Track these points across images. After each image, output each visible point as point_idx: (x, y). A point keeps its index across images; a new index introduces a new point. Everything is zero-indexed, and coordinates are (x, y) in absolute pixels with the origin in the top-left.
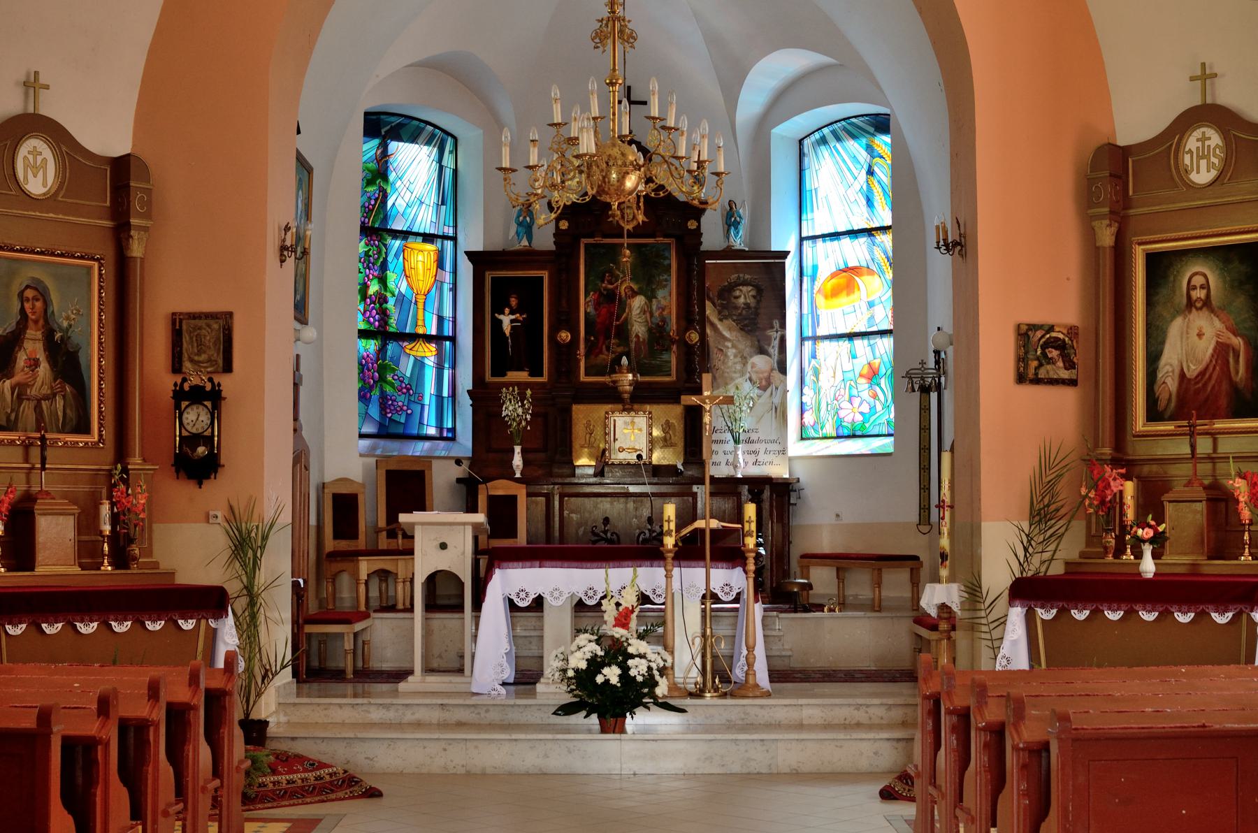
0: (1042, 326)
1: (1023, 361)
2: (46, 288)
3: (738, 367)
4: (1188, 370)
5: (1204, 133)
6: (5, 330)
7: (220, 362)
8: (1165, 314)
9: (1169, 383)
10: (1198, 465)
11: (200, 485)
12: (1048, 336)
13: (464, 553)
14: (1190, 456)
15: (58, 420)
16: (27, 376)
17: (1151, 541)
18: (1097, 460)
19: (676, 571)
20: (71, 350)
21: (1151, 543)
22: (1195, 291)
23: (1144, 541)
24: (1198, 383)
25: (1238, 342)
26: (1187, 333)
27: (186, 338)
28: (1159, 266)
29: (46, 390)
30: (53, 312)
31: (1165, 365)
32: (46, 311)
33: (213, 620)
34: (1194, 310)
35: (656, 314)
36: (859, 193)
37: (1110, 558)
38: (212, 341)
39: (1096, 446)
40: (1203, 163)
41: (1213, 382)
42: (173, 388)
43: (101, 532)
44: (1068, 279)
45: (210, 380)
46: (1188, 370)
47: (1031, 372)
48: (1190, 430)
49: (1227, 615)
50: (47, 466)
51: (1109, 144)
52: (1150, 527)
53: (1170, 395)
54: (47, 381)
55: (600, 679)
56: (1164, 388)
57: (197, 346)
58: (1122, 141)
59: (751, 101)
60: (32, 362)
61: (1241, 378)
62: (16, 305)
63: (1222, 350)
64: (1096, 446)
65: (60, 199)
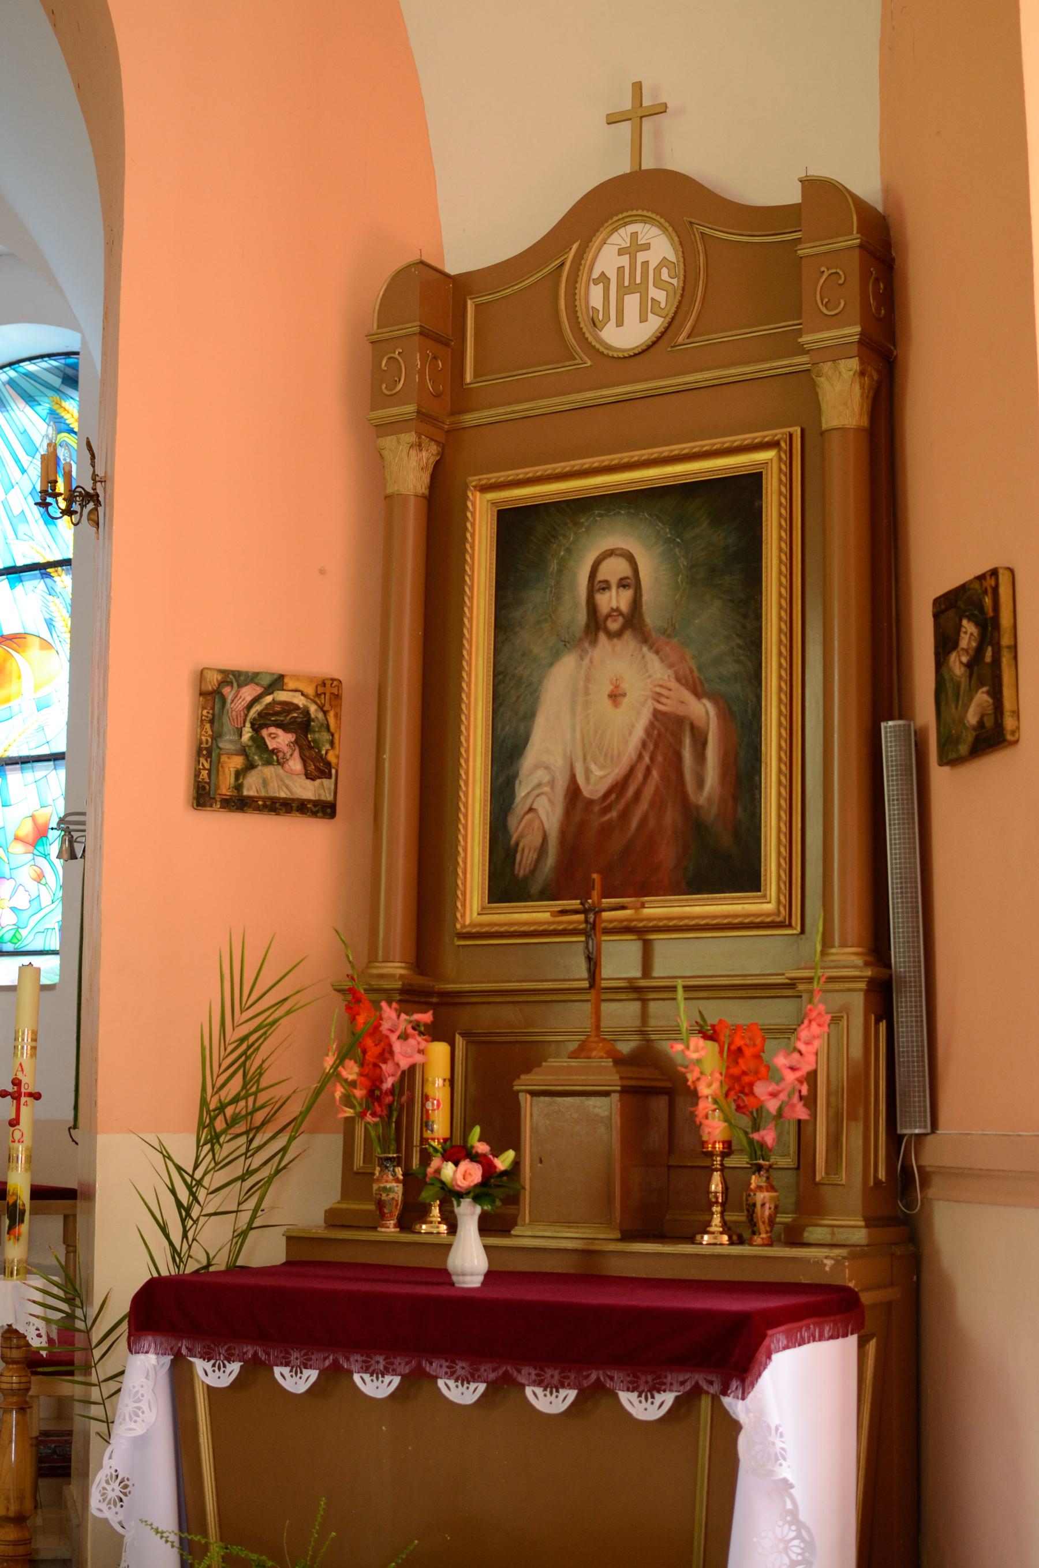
0: (257, 674)
1: (209, 755)
4: (587, 779)
5: (634, 235)
8: (536, 650)
10: (604, 1006)
12: (269, 699)
14: (585, 984)
17: (479, 1194)
18: (370, 990)
21: (477, 1199)
22: (607, 594)
23: (460, 1195)
24: (606, 810)
26: (587, 693)
31: (536, 767)
34: (602, 637)
36: (30, 497)
37: (390, 1229)
39: (372, 959)
40: (632, 302)
41: (644, 805)
44: (322, 572)
46: (587, 779)
47: (226, 784)
48: (586, 921)
49: (659, 1397)
51: (422, 263)
52: (474, 1157)
53: (545, 838)
56: (531, 821)
58: (453, 268)
61: (709, 800)
64: (372, 959)
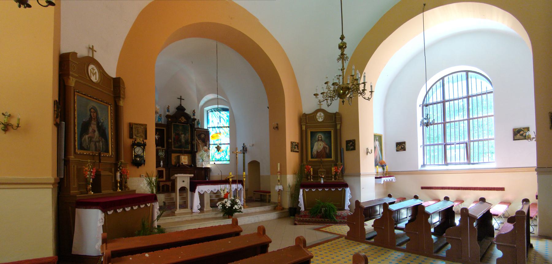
3: (202, 148)
7: (144, 137)
9: (315, 152)
13: (188, 183)
19: (238, 185)
25: (327, 146)
27: (134, 130)
28: (313, 134)
29: (97, 140)
30: (99, 117)
32: (97, 116)
35: (186, 138)
38: (141, 131)
40: (320, 118)
55: (234, 208)
59: (202, 103)
62: (89, 113)
63: (324, 148)
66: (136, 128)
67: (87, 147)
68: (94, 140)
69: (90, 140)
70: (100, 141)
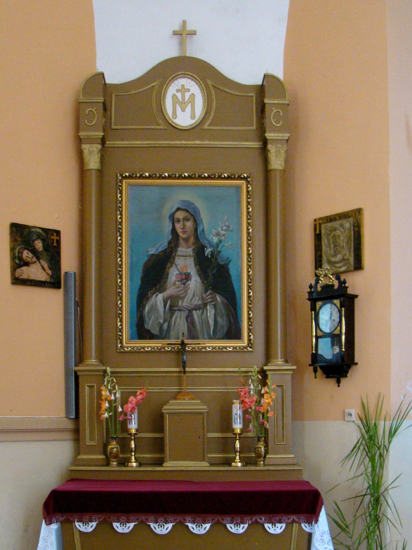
2: (196, 210)
6: (157, 249)
7: (352, 260)
11: (338, 382)
15: (209, 327)
16: (179, 289)
20: (222, 263)
29: (197, 301)
30: (203, 230)
32: (196, 230)
33: (307, 525)
38: (345, 240)
42: (309, 290)
43: (233, 430)
45: (338, 278)
50: (187, 369)
54: (198, 292)
57: (334, 248)
60: (184, 276)
62: (168, 227)
65: (206, 127)
66: (331, 231)
67: (161, 326)
68: (185, 303)
69: (171, 306)
70: (205, 305)
